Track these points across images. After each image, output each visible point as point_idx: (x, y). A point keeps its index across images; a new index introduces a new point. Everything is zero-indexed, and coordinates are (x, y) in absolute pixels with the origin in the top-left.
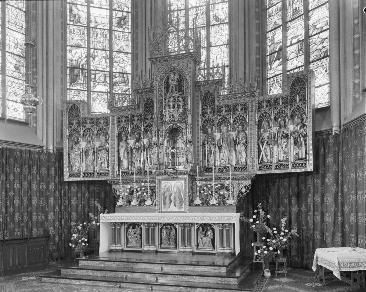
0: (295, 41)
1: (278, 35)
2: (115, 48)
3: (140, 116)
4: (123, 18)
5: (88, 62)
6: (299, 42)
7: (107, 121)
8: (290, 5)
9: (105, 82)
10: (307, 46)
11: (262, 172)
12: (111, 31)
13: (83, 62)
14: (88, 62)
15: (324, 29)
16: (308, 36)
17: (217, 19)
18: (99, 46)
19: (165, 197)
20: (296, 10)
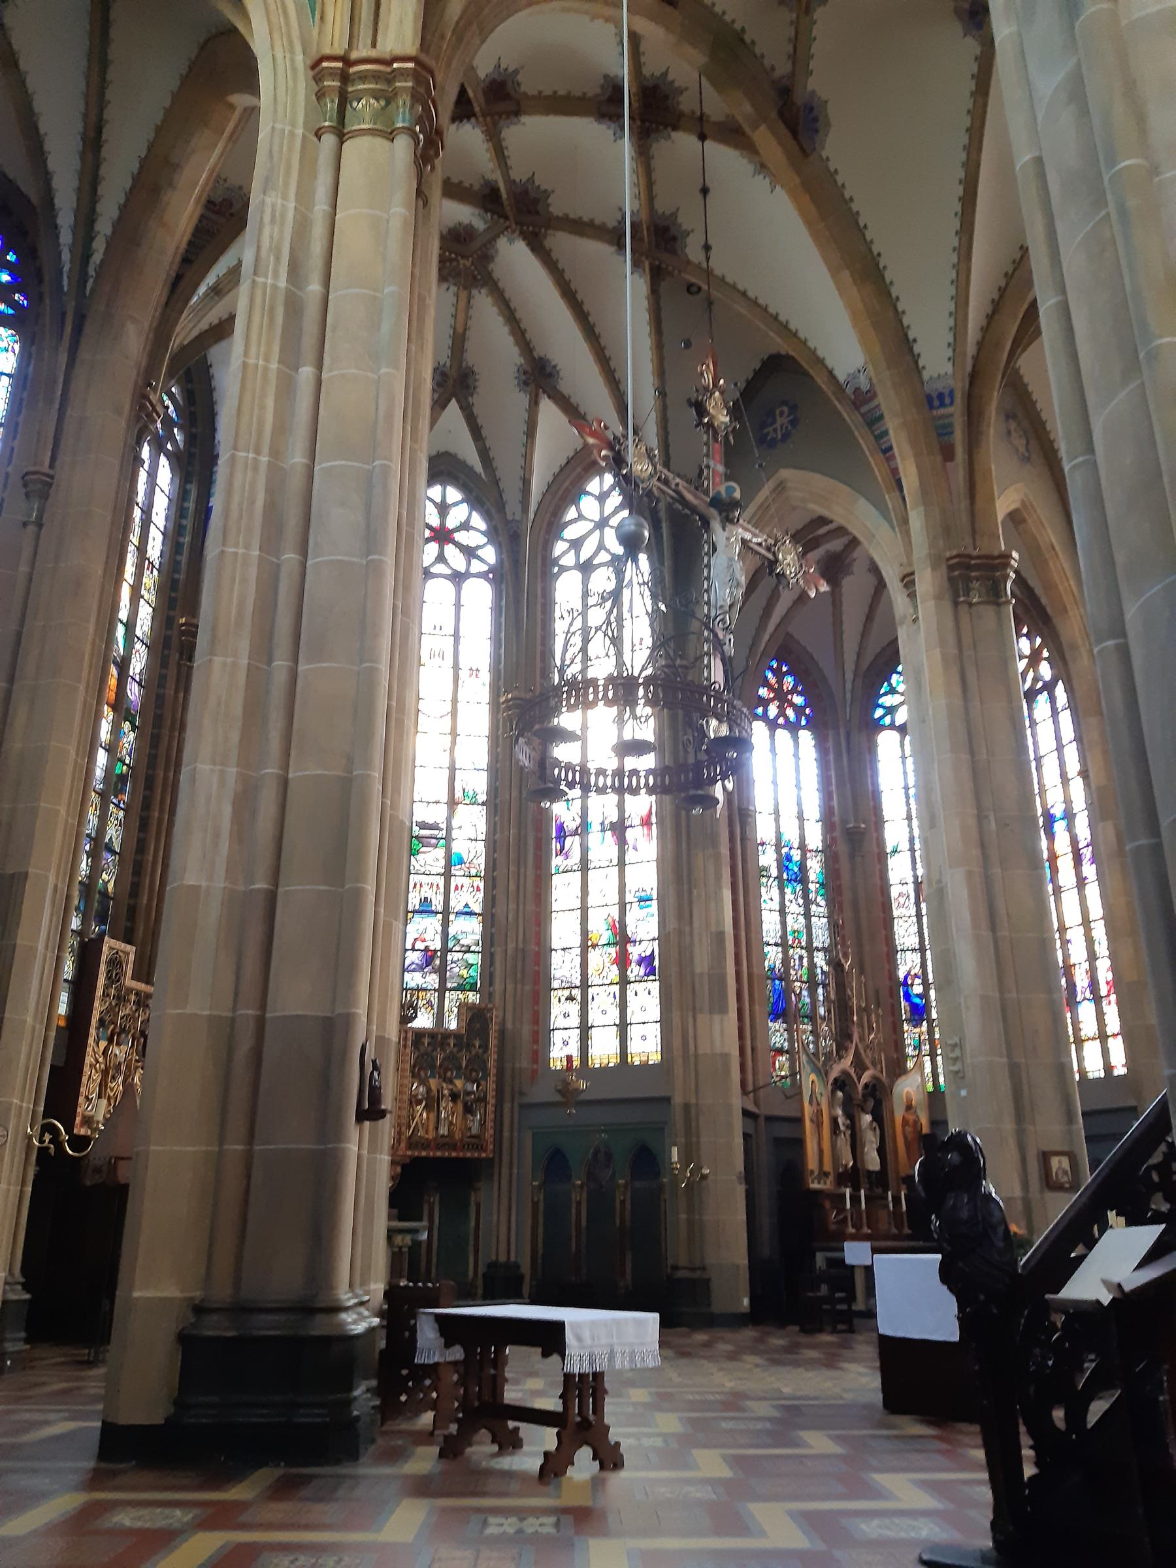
0: (420, 945)
6: (427, 949)
8: (415, 887)
15: (473, 948)
16: (446, 950)
20: (425, 901)
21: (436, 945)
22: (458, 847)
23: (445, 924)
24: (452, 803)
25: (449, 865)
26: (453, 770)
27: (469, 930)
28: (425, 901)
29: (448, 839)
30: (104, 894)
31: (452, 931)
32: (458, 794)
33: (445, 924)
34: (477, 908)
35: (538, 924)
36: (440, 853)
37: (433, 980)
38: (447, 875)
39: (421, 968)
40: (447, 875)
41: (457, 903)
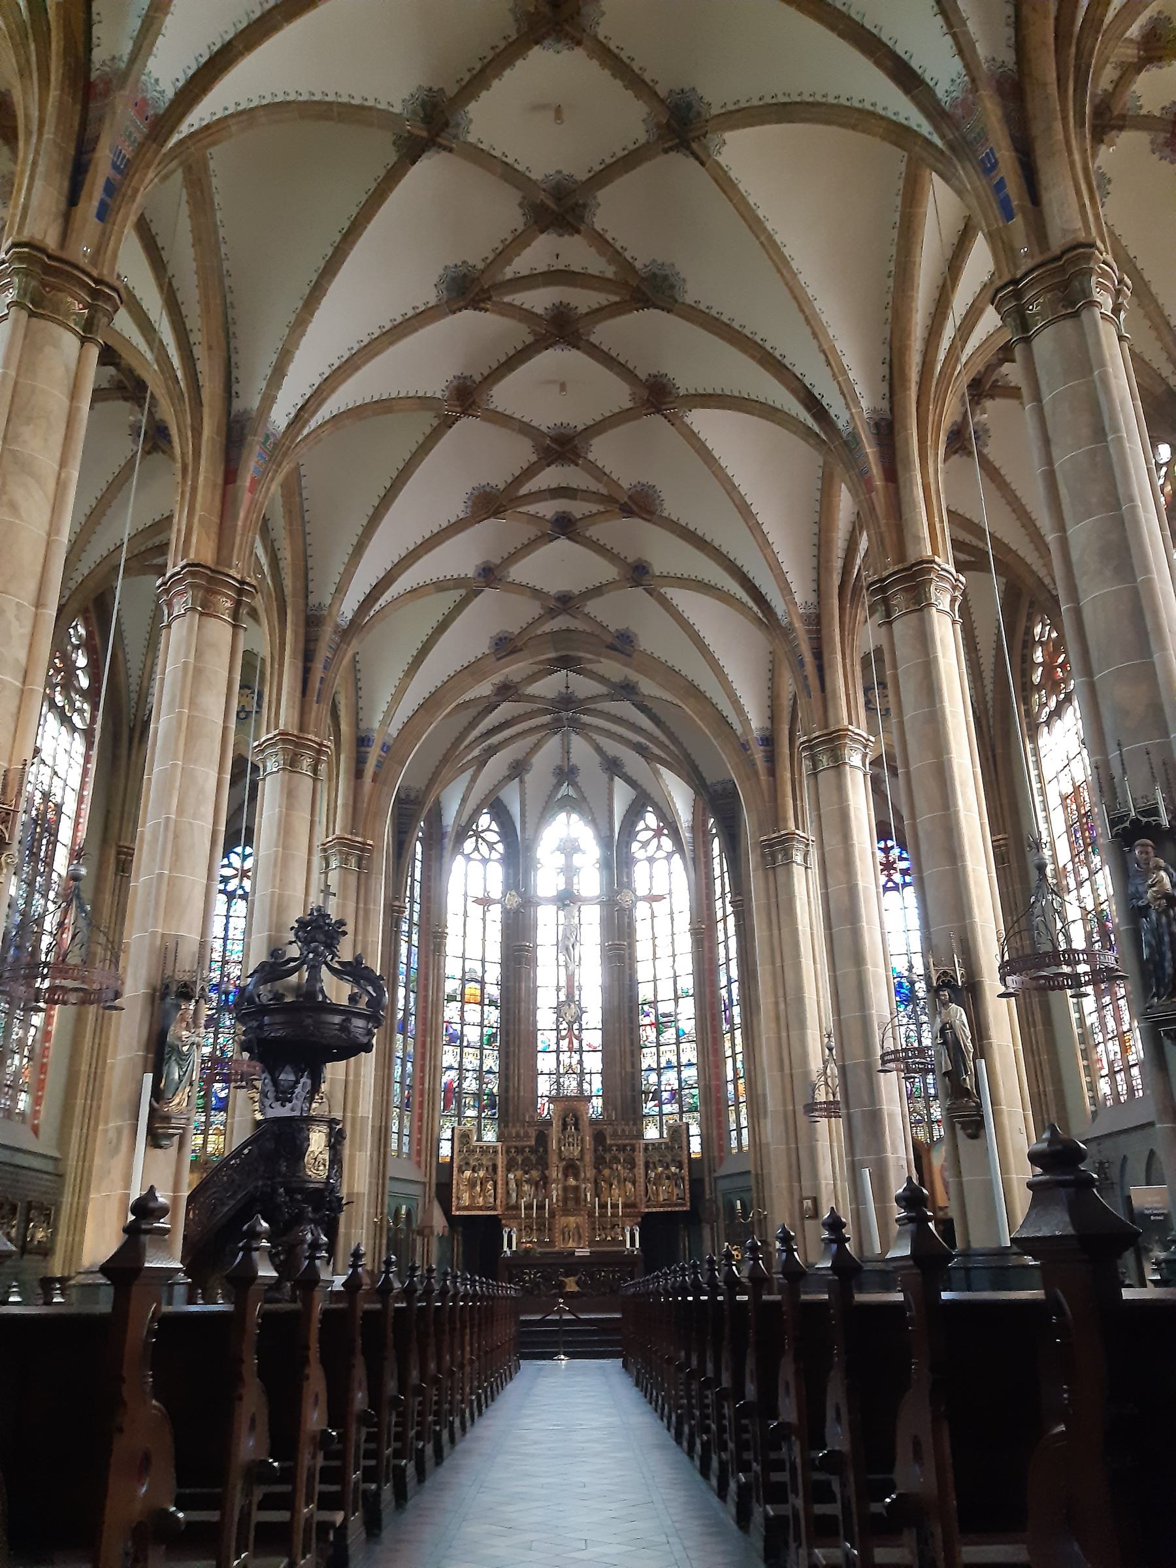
0: (669, 1088)
1: (653, 1078)
2: (485, 1068)
3: (530, 1147)
4: (494, 1035)
5: (460, 1085)
7: (495, 1152)
9: (474, 1106)
10: (681, 1096)
11: (650, 1210)
12: (481, 1049)
13: (455, 1085)
14: (460, 1085)
16: (681, 1088)
17: (589, 1045)
18: (469, 1067)
19: (564, 1234)
20: (669, 1062)
21: (676, 1087)
22: (681, 1025)
23: (679, 1073)
24: (676, 999)
25: (678, 1036)
26: (675, 977)
27: (690, 1074)
28: (669, 1062)
29: (677, 1021)
30: (491, 1095)
31: (683, 1076)
32: (679, 992)
33: (679, 1073)
34: (694, 1061)
35: (717, 1067)
36: (672, 1031)
37: (676, 1107)
38: (678, 1043)
39: (670, 1102)
40: (678, 1043)
41: (684, 1061)
